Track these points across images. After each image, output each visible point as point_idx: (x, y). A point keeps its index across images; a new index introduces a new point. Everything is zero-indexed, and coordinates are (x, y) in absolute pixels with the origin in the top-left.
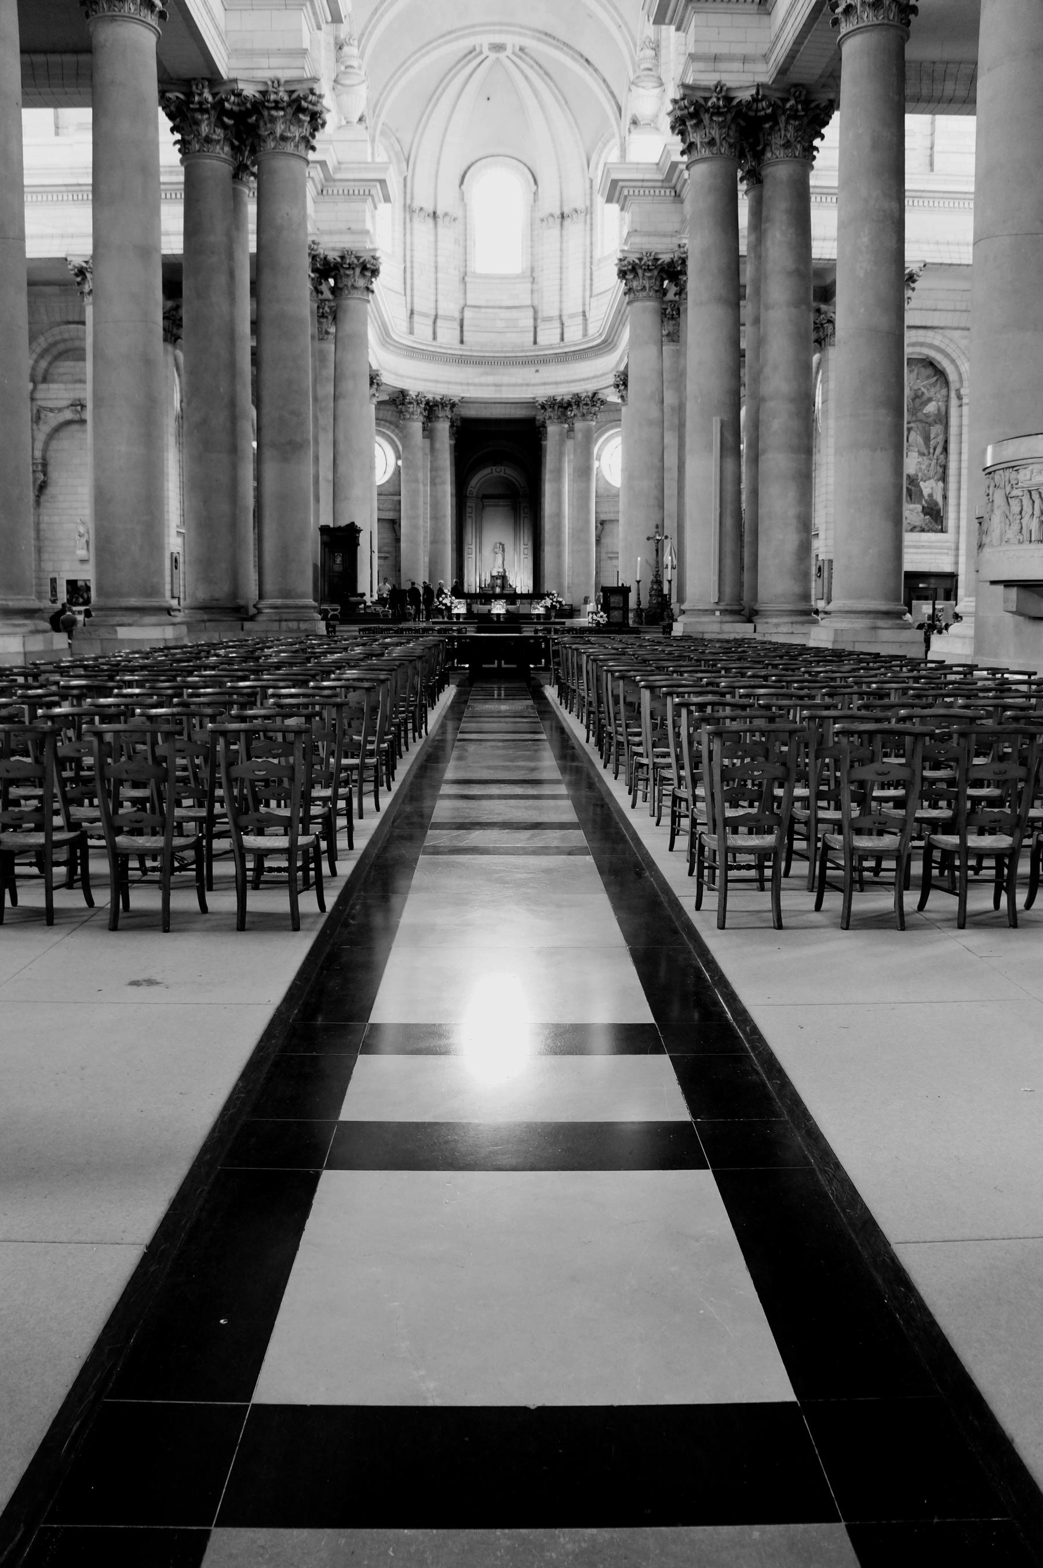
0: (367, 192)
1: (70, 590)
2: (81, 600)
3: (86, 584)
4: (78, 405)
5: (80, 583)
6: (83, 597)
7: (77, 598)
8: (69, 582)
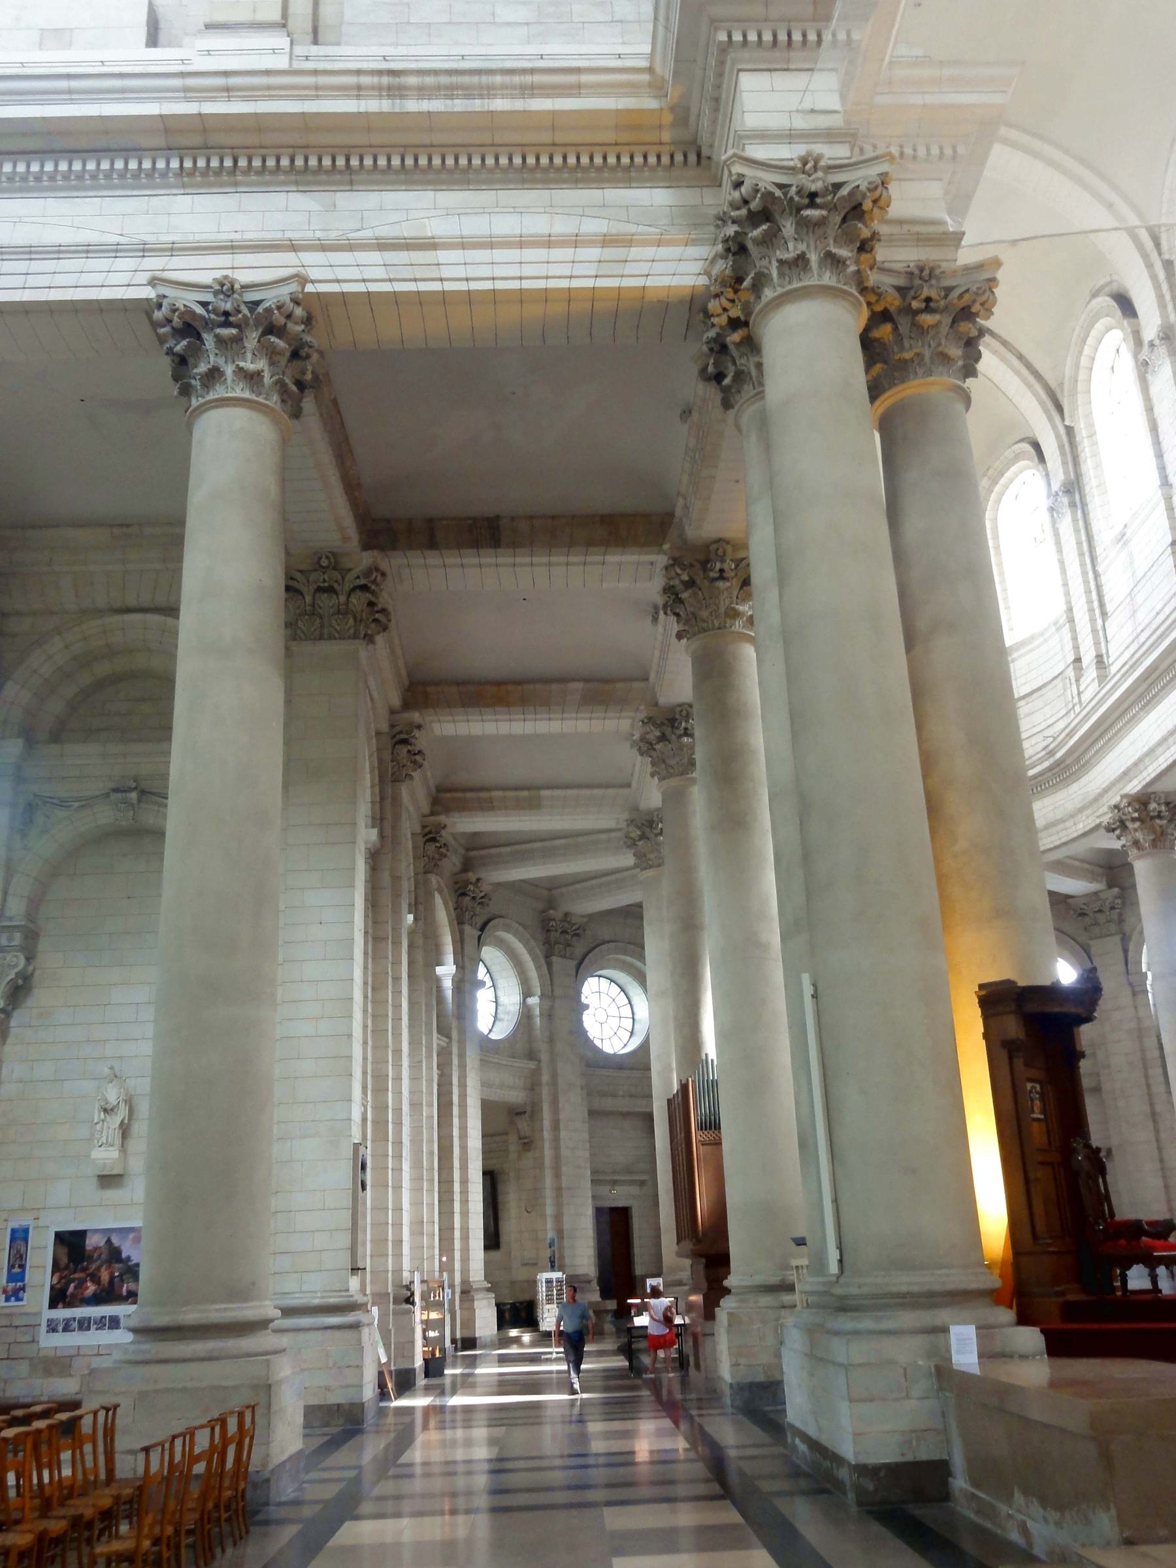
0: (948, 152)
1: (64, 1260)
2: (91, 1288)
3: (109, 1241)
4: (131, 790)
5: (92, 1242)
6: (95, 1278)
7: (81, 1284)
8: (60, 1237)
